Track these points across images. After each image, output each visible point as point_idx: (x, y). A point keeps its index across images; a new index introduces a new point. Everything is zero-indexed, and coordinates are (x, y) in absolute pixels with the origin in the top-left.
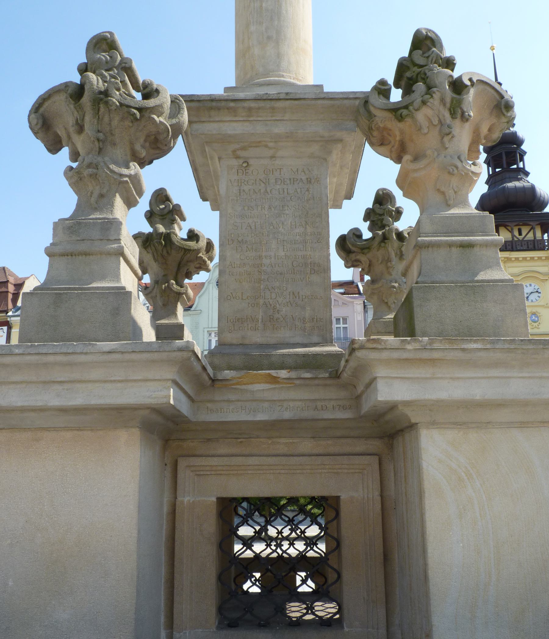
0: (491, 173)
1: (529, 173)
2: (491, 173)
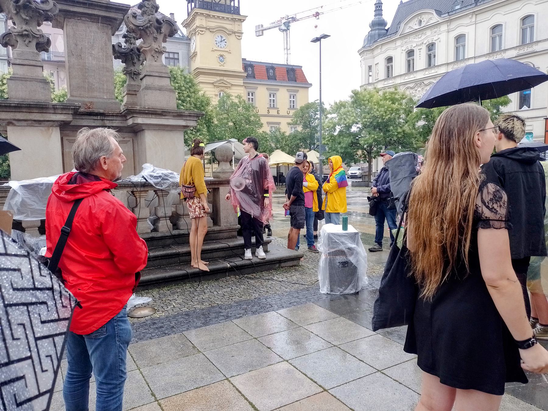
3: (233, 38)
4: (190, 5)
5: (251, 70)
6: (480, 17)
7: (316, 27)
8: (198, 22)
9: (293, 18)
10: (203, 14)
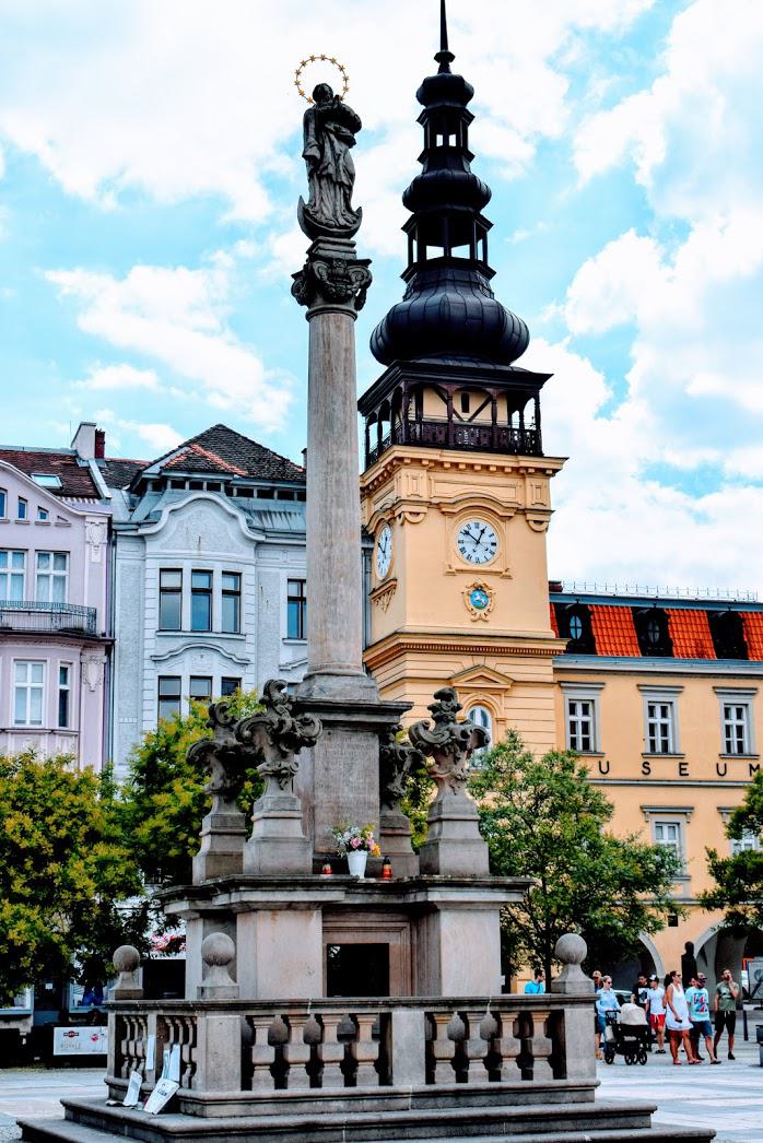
0: (415, 260)
1: (494, 273)
2: (415, 260)
3: (518, 526)
4: (374, 428)
5: (578, 621)
10: (420, 460)
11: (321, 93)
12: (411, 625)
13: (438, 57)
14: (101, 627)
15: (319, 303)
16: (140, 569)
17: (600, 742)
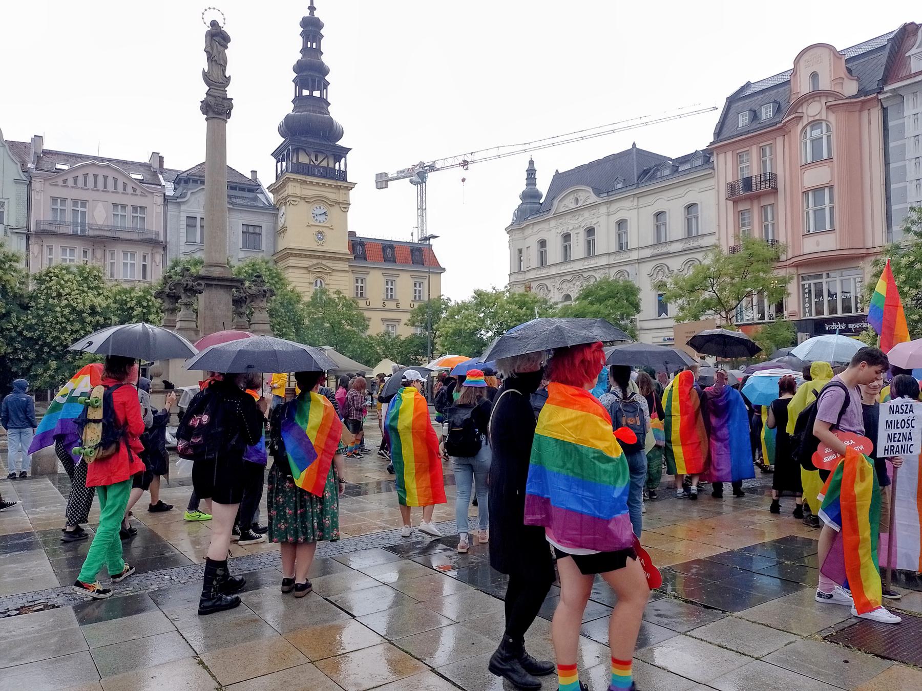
3: (336, 210)
4: (279, 164)
6: (643, 201)
7: (464, 180)
8: (291, 189)
9: (430, 166)
11: (214, 24)
12: (292, 245)
13: (309, 8)
14: (161, 238)
15: (211, 115)
16: (178, 218)
17: (368, 294)
